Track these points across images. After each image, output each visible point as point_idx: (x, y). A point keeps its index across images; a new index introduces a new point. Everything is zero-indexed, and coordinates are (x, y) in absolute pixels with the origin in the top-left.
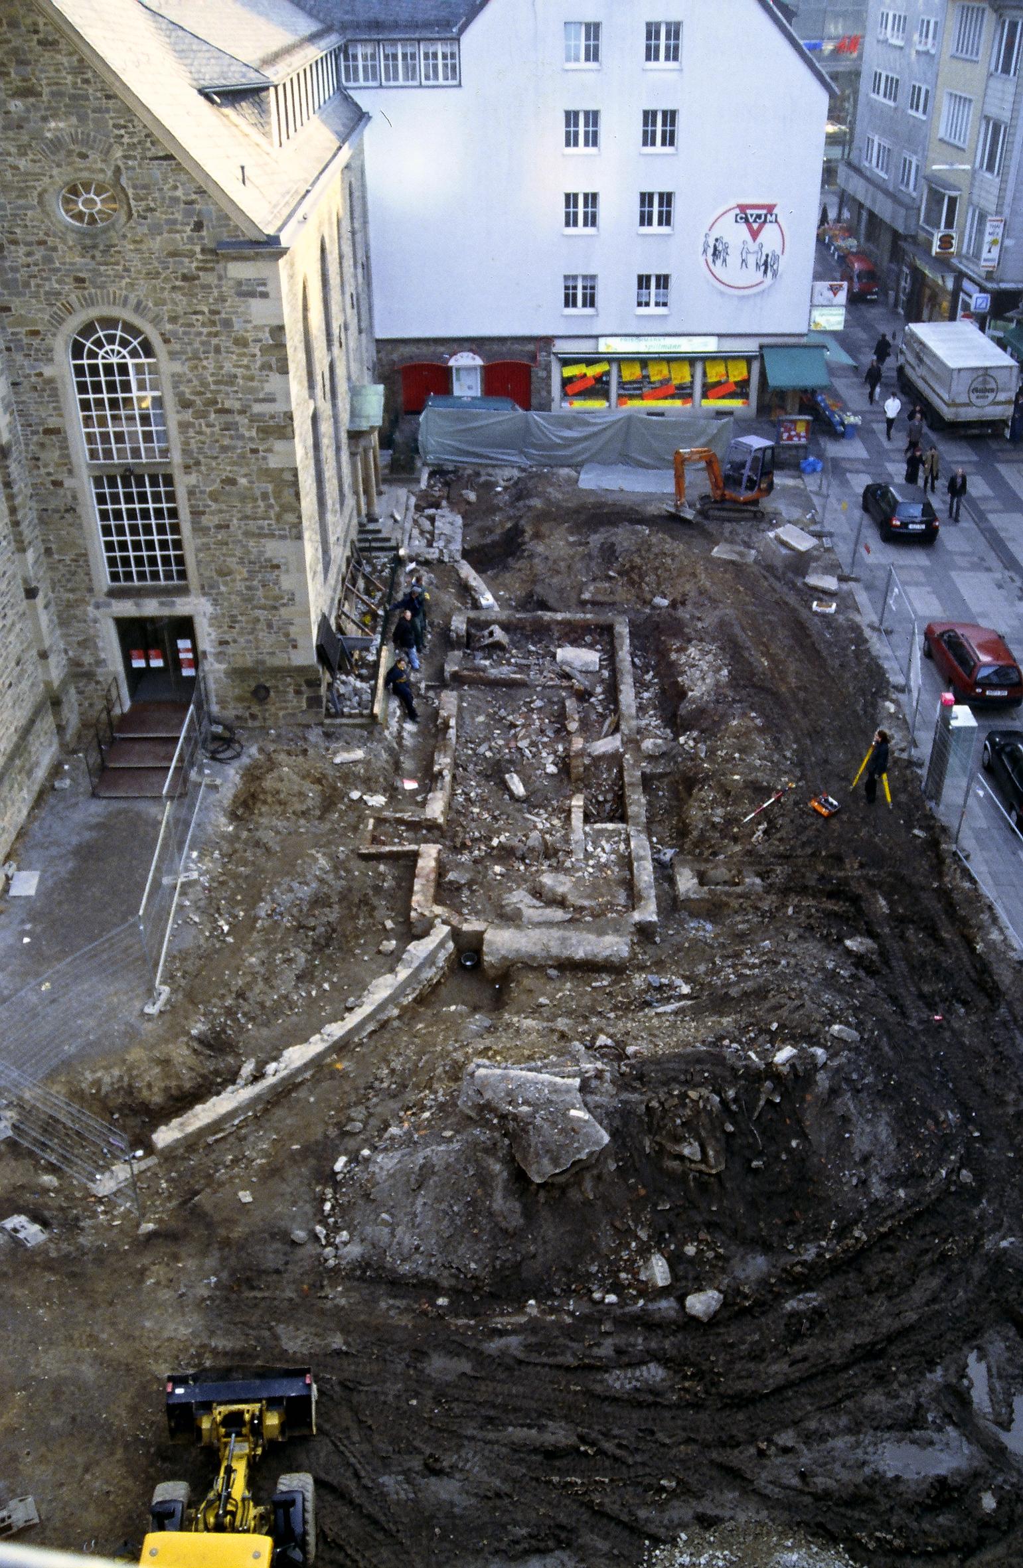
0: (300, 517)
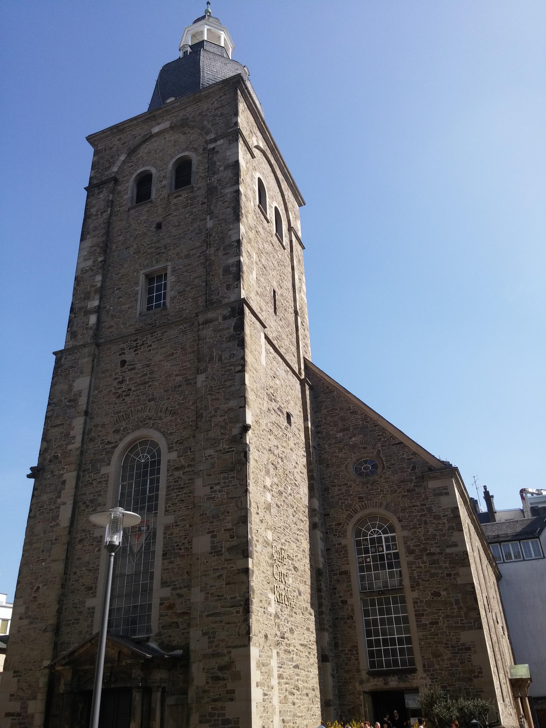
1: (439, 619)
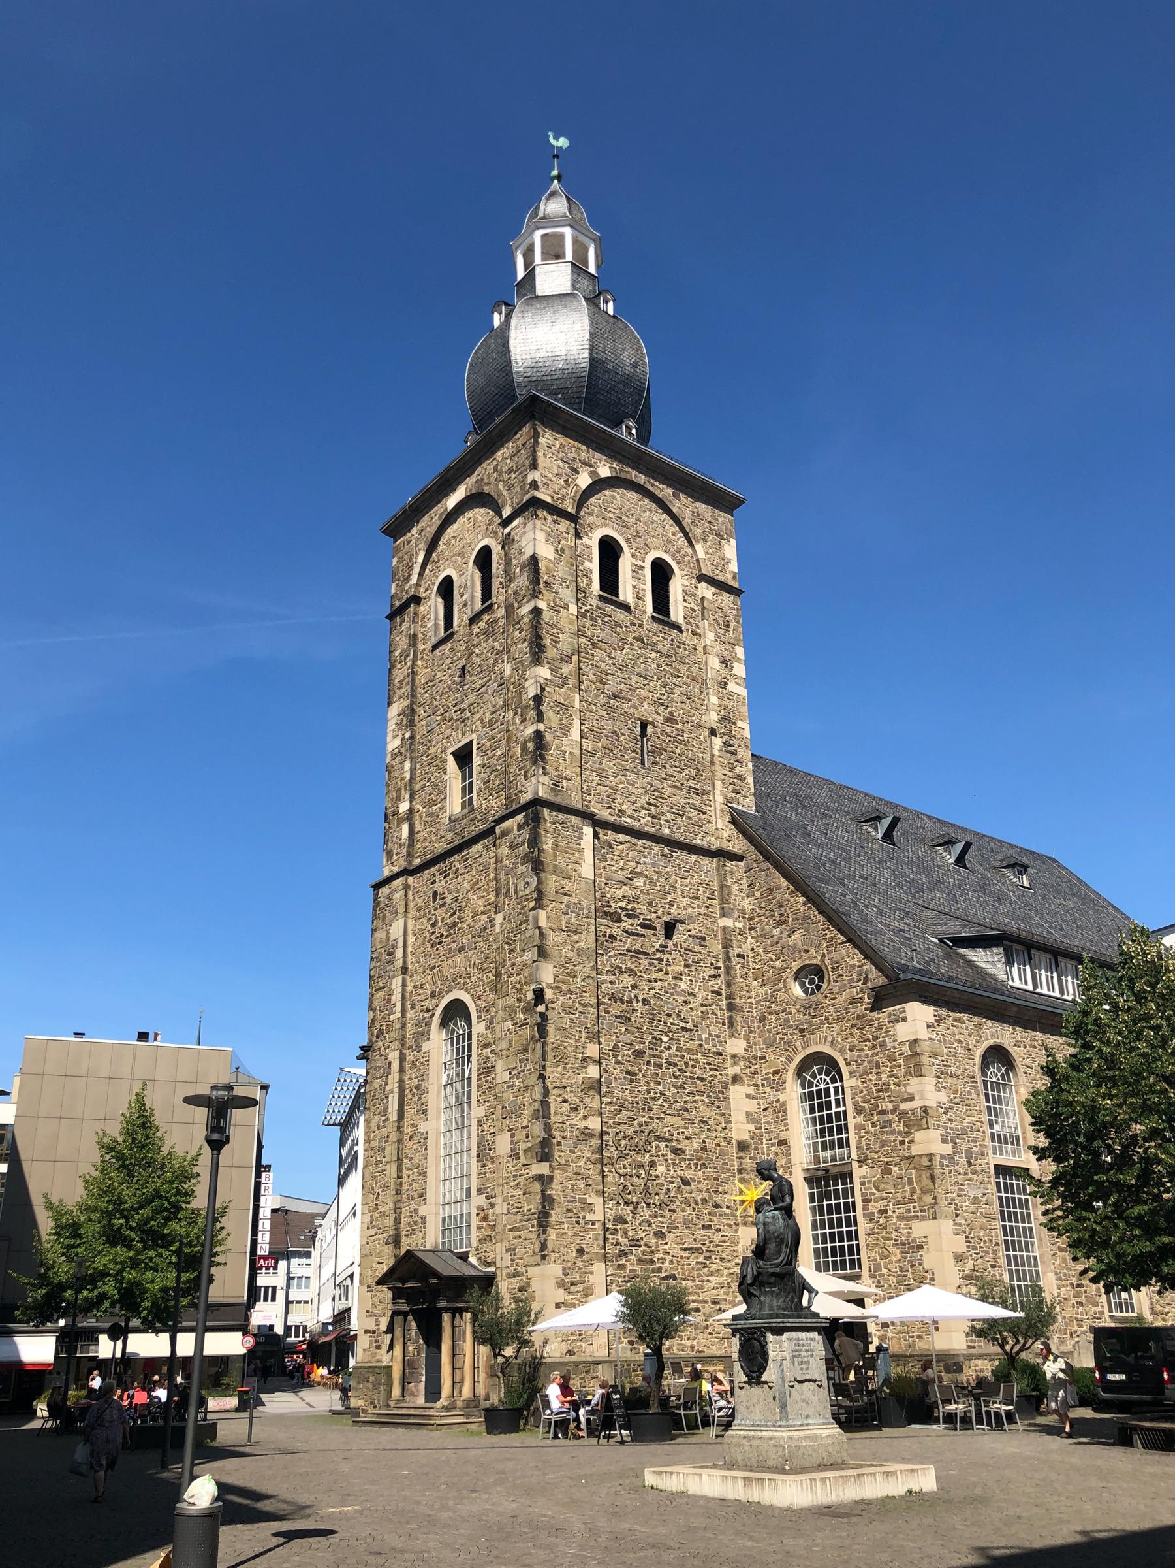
1: (888, 1205)
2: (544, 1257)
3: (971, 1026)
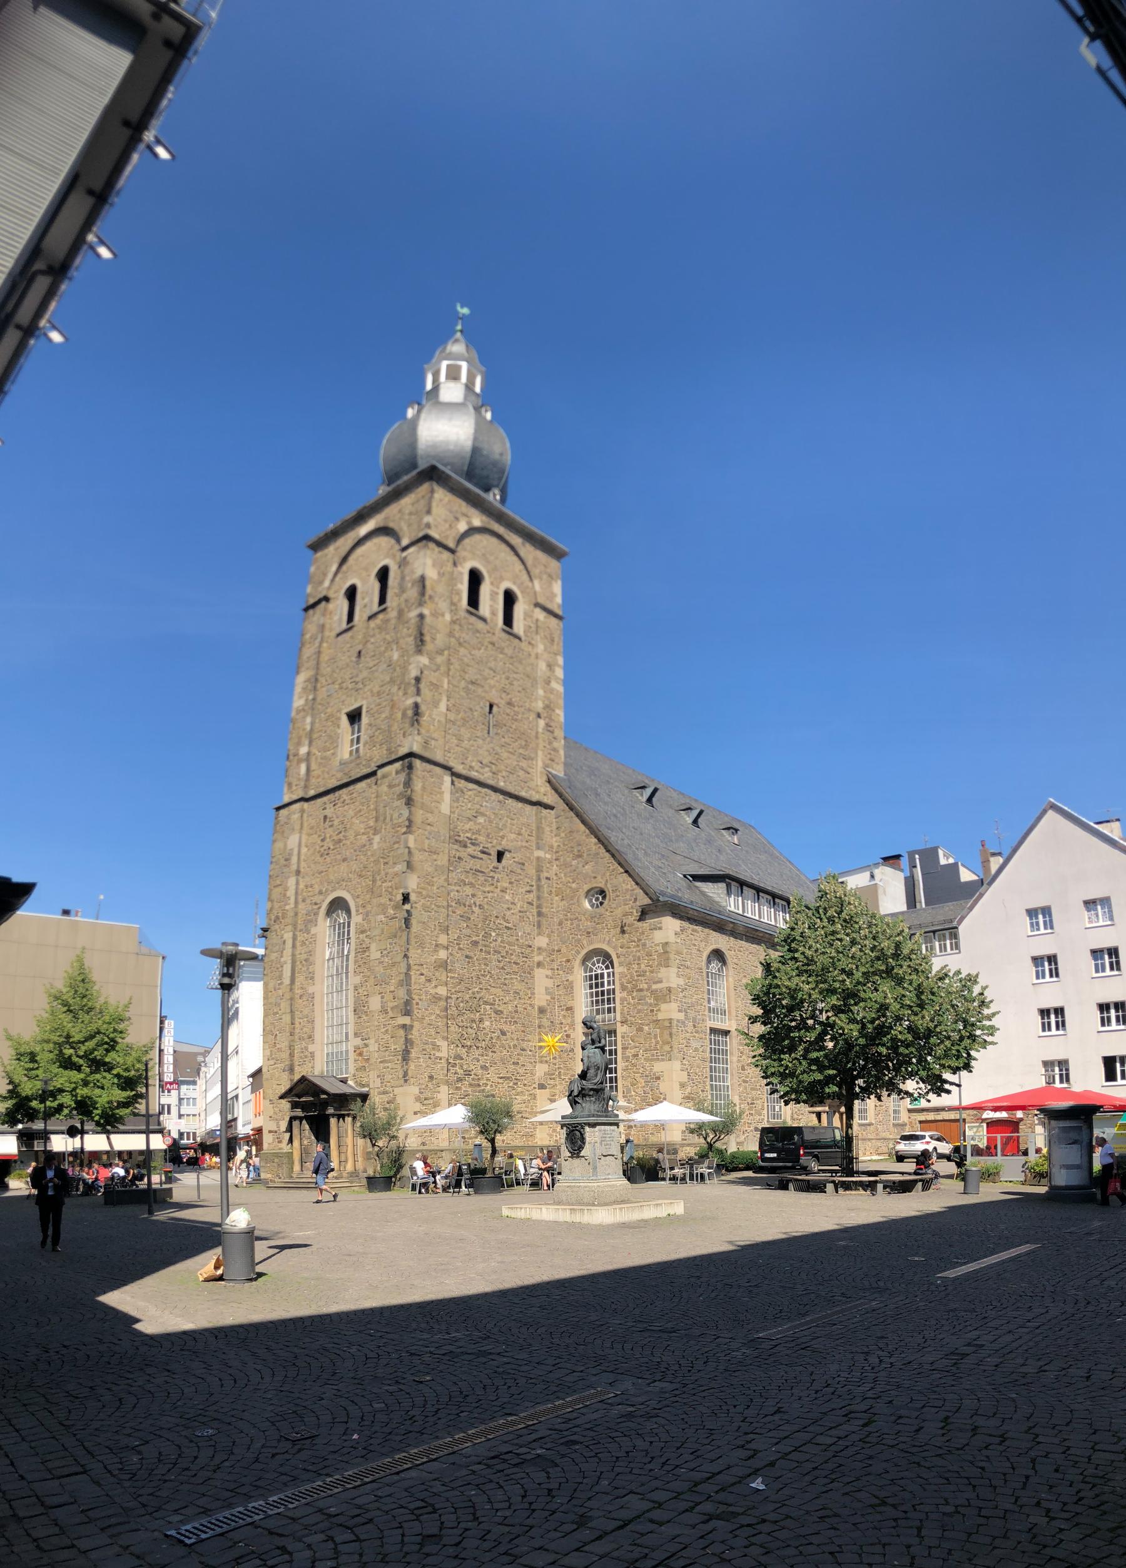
0: (671, 1047)
2: (406, 1081)
3: (703, 935)
